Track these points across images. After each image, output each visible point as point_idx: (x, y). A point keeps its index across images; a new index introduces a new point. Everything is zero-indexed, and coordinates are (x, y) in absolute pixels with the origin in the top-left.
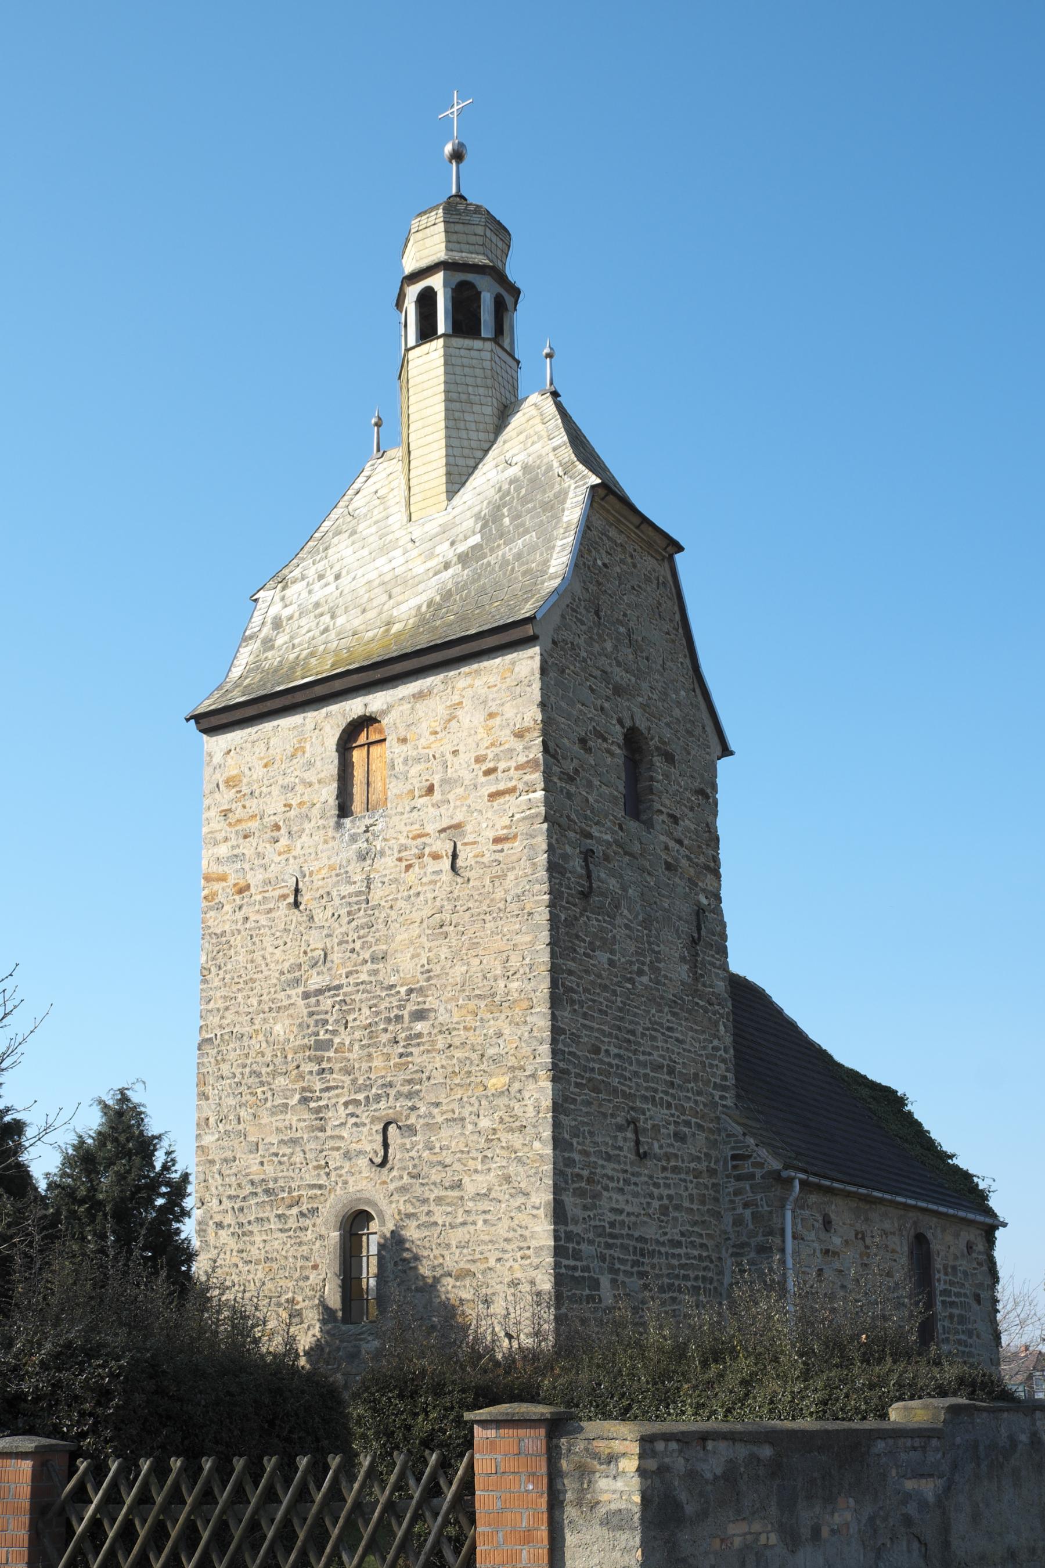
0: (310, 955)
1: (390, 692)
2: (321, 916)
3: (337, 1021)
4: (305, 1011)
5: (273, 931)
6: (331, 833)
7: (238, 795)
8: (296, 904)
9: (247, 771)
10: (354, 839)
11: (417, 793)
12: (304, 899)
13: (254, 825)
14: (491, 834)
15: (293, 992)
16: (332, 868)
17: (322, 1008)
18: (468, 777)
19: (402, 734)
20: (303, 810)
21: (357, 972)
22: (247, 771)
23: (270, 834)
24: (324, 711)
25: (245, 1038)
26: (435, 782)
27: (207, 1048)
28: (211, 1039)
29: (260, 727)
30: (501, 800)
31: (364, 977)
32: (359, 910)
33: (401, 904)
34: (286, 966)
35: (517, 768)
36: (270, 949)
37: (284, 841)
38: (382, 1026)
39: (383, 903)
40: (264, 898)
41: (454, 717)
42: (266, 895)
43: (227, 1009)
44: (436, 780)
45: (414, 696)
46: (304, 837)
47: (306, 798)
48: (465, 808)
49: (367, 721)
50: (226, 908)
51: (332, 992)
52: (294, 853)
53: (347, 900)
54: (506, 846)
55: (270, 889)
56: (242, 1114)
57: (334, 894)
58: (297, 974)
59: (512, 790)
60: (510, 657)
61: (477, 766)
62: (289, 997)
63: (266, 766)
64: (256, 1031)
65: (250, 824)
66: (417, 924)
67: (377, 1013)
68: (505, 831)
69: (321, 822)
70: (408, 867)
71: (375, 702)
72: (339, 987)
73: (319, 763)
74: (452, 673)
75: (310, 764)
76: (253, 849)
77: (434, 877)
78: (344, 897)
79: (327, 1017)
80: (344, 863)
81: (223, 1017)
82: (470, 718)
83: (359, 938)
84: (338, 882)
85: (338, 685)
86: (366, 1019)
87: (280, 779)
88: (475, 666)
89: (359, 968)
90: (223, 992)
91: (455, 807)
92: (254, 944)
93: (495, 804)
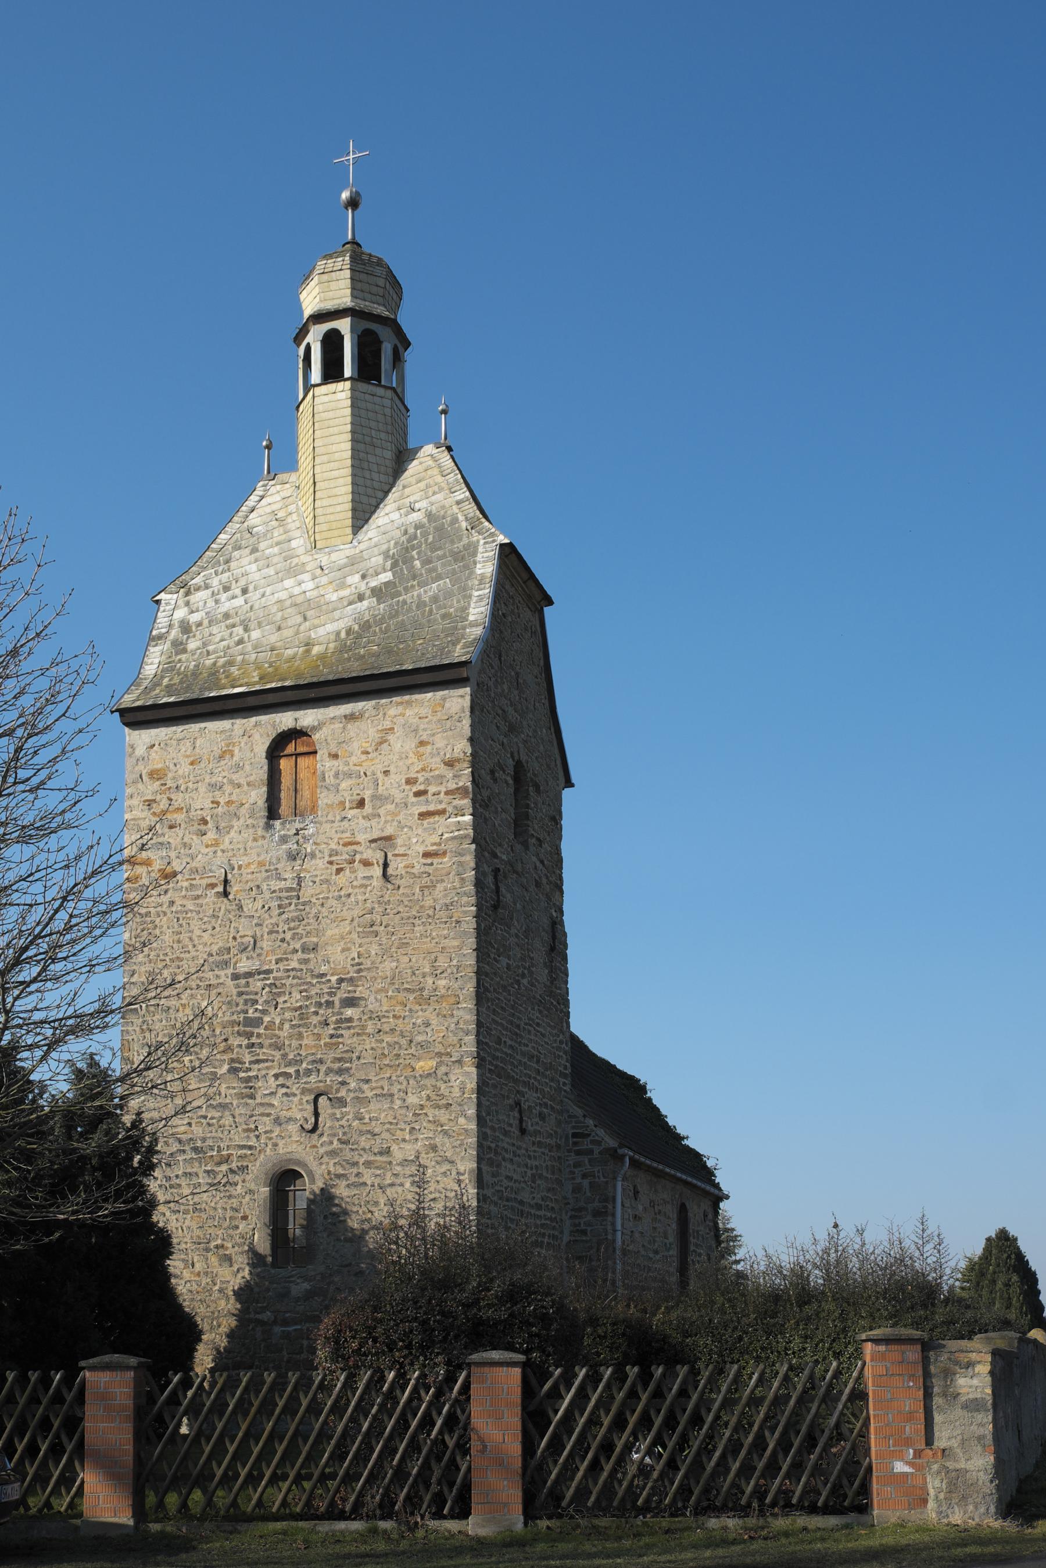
0: (239, 940)
1: (322, 710)
2: (250, 906)
3: (267, 1002)
4: (235, 992)
5: (201, 916)
6: (260, 832)
7: (163, 788)
8: (226, 894)
9: (172, 766)
10: (284, 839)
11: (347, 805)
12: (233, 889)
13: (180, 817)
14: (421, 849)
15: (222, 973)
16: (261, 864)
17: (251, 988)
18: (398, 796)
19: (334, 751)
20: (231, 809)
21: (287, 959)
22: (172, 766)
23: (196, 827)
24: (253, 719)
25: (171, 1011)
26: (366, 797)
29: (187, 727)
30: (431, 820)
31: (294, 964)
32: (290, 904)
33: (334, 903)
34: (215, 949)
35: (447, 793)
36: (197, 932)
37: (211, 835)
38: (313, 1010)
39: (314, 900)
40: (191, 885)
41: (386, 741)
42: (194, 882)
44: (367, 795)
45: (345, 717)
46: (232, 833)
47: (234, 798)
48: (395, 823)
51: (262, 976)
52: (222, 847)
53: (277, 894)
54: (436, 861)
55: (198, 877)
57: (264, 887)
58: (226, 957)
59: (443, 812)
60: (441, 693)
61: (408, 787)
62: (218, 977)
63: (192, 764)
64: (184, 1006)
65: (175, 816)
66: (347, 922)
67: (308, 998)
68: (435, 847)
69: (250, 822)
70: (339, 871)
71: (307, 717)
72: (268, 972)
73: (247, 767)
74: (384, 701)
75: (238, 767)
76: (179, 839)
77: (364, 882)
78: (274, 891)
79: (256, 997)
80: (274, 861)
82: (400, 744)
83: (290, 929)
84: (268, 877)
85: (271, 699)
86: (297, 1002)
88: (407, 697)
89: (289, 956)
91: (386, 822)
92: (181, 926)
93: (425, 822)
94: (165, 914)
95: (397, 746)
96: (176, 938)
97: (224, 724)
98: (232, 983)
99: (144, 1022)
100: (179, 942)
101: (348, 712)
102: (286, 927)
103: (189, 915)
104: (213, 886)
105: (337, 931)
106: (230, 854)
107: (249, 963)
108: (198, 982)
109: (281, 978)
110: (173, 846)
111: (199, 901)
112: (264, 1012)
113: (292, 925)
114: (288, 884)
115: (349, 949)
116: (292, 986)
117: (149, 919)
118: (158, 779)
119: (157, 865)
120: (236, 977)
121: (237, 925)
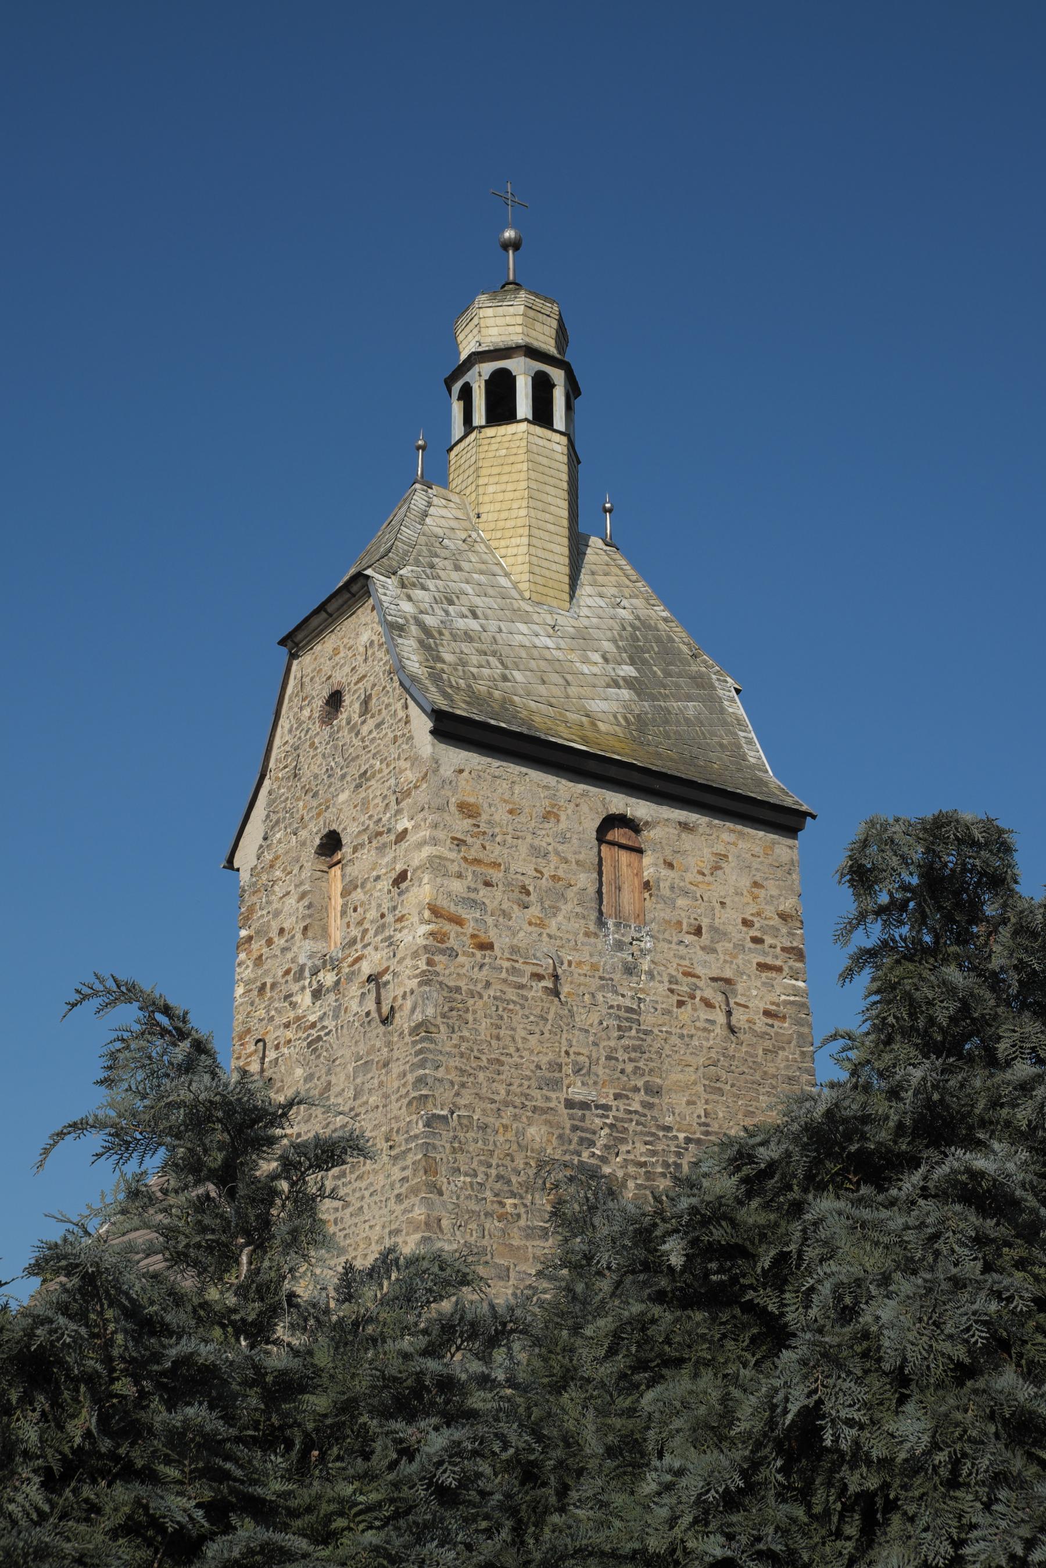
0: (572, 1056)
2: (584, 1017)
3: (606, 1147)
4: (568, 1125)
6: (592, 927)
7: (476, 830)
8: (556, 993)
9: (486, 805)
10: (619, 946)
11: (685, 927)
12: (565, 989)
13: (496, 876)
14: (762, 1006)
16: (594, 967)
17: (587, 1124)
18: (736, 937)
19: (669, 858)
20: (558, 886)
21: (627, 1097)
22: (486, 805)
23: (516, 895)
24: (582, 787)
25: (489, 1130)
26: (703, 925)
27: (440, 1128)
28: (444, 1118)
29: (504, 764)
30: (769, 974)
31: (636, 1106)
32: (631, 1028)
33: (678, 1041)
34: (544, 1060)
35: (783, 949)
36: (521, 1033)
37: (534, 911)
38: (660, 1170)
39: (656, 1031)
40: (514, 968)
41: (720, 868)
42: (516, 965)
43: (463, 1085)
44: (705, 923)
45: (680, 823)
46: (560, 918)
47: (560, 873)
48: (734, 966)
49: (631, 824)
50: (461, 959)
51: (600, 1112)
52: (548, 931)
54: (776, 1023)
55: (521, 961)
56: (487, 1226)
57: (600, 998)
58: (557, 1075)
59: (779, 969)
61: (744, 929)
62: (548, 1099)
63: (511, 812)
64: (505, 1127)
65: (491, 871)
66: (692, 1069)
67: (654, 1153)
68: (774, 1008)
69: (578, 909)
70: (680, 1004)
71: (640, 809)
72: (606, 1107)
74: (716, 822)
76: (496, 903)
78: (611, 1007)
79: (595, 1138)
81: (457, 1094)
82: (733, 878)
83: (631, 1060)
84: (603, 986)
85: (613, 772)
86: (641, 1155)
87: (529, 837)
88: (739, 827)
89: (630, 1094)
90: (457, 1062)
91: (725, 961)
92: (501, 1018)
93: (764, 975)
94: (481, 997)
95: (732, 878)
96: (495, 1032)
97: (550, 780)
98: (566, 1111)
99: (455, 1137)
100: (498, 1038)
101: (682, 819)
102: (626, 1056)
103: (511, 1006)
104: (539, 977)
105: (680, 1076)
106: (558, 942)
107: (584, 1090)
108: (523, 1099)
109: (622, 1120)
110: (489, 909)
111: (524, 992)
112: (604, 1160)
113: (633, 1055)
114: (628, 1003)
115: (694, 1103)
116: (635, 1133)
117: (457, 996)
118: (470, 816)
119: (470, 928)
120: (570, 1104)
121: (570, 1037)
